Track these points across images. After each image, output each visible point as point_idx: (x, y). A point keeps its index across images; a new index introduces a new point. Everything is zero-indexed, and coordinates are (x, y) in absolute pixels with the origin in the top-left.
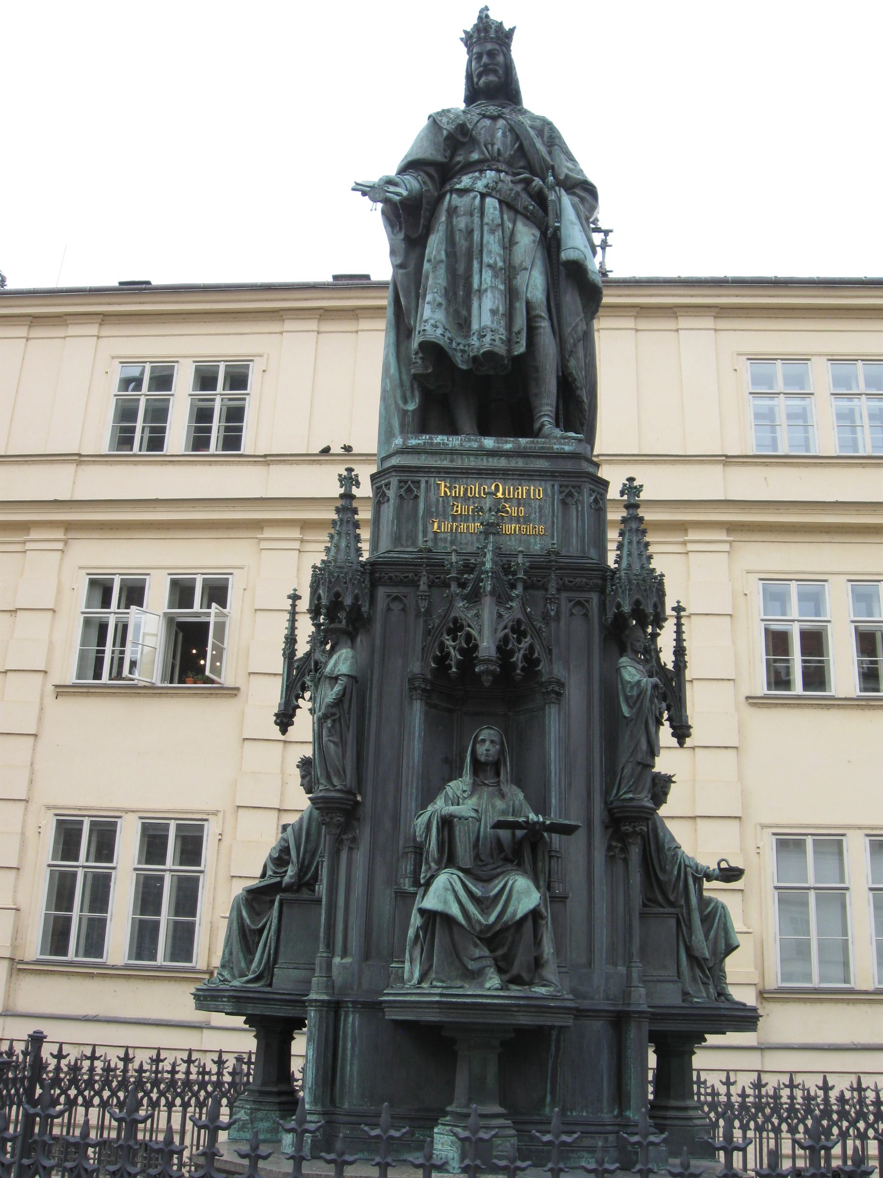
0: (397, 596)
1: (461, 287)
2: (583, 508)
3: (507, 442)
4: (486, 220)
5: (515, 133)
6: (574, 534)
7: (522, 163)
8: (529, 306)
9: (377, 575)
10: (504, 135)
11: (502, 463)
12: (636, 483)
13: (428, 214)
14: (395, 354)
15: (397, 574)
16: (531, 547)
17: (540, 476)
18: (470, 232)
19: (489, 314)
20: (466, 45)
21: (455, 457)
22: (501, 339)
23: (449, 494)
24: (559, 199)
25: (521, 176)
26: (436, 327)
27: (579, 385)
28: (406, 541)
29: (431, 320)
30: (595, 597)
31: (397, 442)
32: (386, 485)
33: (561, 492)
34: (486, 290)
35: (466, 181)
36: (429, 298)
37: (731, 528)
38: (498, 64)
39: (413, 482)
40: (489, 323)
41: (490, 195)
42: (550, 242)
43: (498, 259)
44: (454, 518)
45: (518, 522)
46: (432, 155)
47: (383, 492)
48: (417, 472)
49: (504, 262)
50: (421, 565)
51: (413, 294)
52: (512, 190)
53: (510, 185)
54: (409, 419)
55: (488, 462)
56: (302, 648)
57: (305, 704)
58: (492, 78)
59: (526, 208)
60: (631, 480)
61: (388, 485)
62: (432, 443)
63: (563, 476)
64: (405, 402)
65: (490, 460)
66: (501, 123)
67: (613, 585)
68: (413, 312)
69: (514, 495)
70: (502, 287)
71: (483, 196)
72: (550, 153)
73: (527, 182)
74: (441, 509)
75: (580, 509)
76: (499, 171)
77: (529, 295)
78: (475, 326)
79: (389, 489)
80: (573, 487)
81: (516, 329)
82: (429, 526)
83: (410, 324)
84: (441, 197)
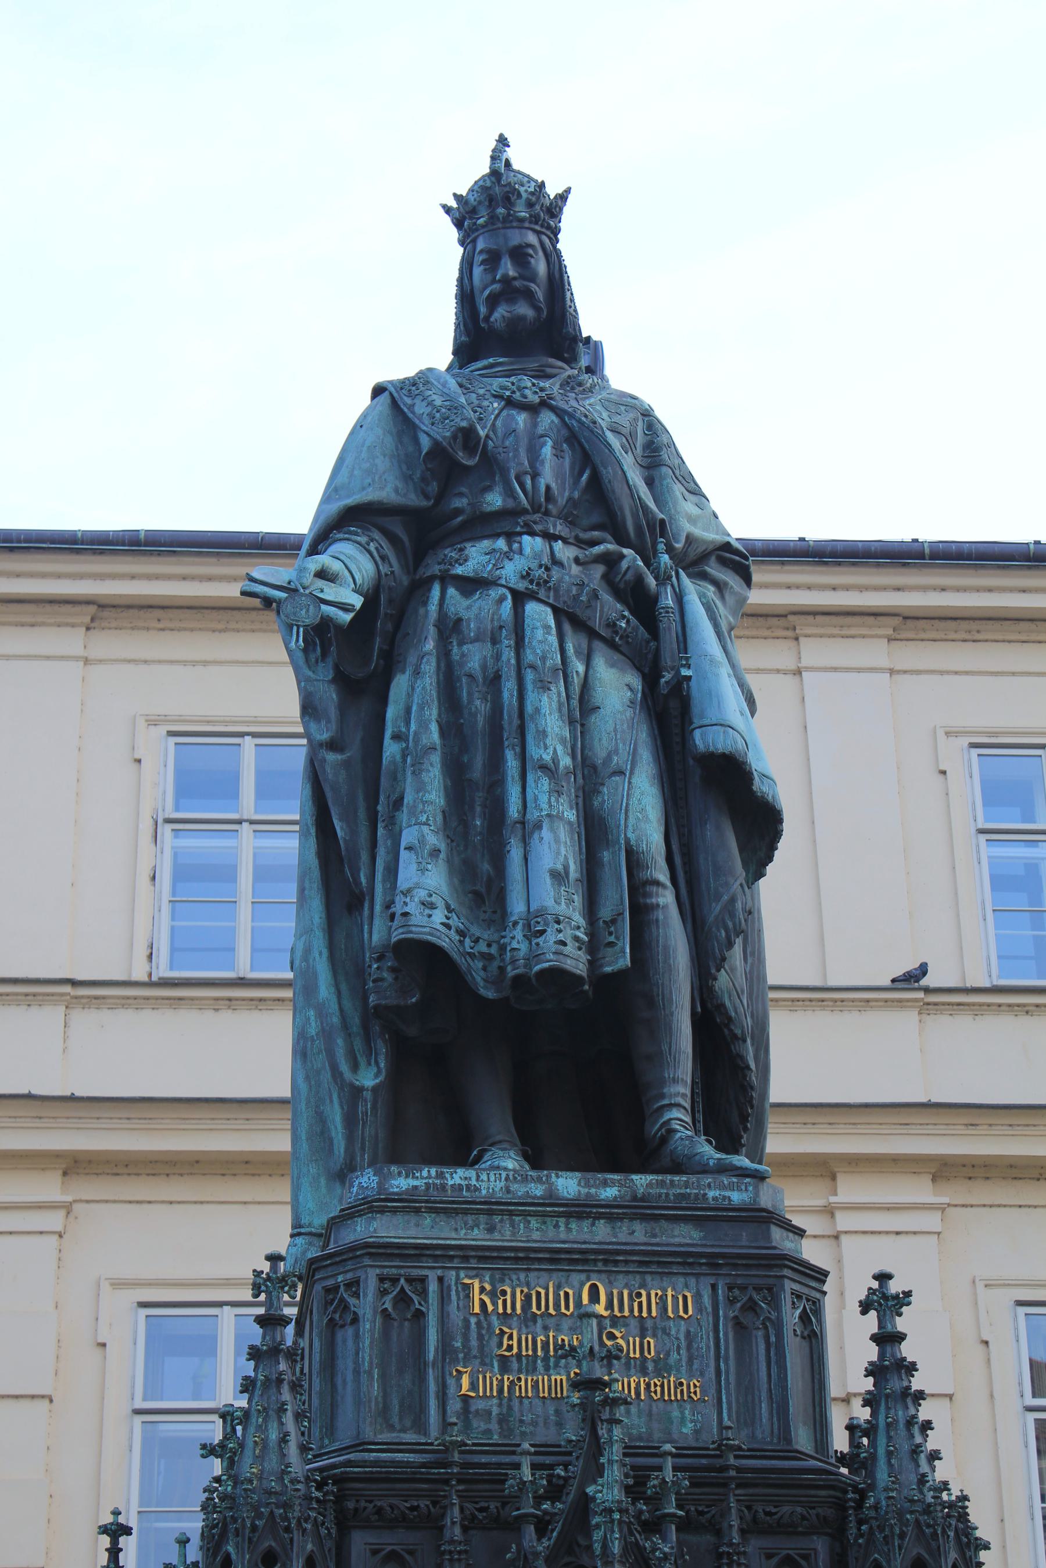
0: (393, 1552)
1: (478, 809)
2: (780, 1336)
3: (605, 1184)
4: (529, 657)
5: (582, 445)
6: (764, 1395)
7: (595, 518)
8: (634, 860)
9: (351, 1505)
10: (558, 454)
11: (601, 1232)
12: (895, 1287)
13: (390, 626)
14: (325, 953)
15: (394, 1501)
16: (674, 1429)
17: (683, 1264)
18: (495, 681)
19: (548, 880)
20: (459, 224)
21: (497, 1219)
22: (576, 939)
23: (490, 1308)
24: (680, 598)
26: (432, 906)
27: (738, 1032)
28: (401, 1419)
29: (424, 892)
30: (820, 1545)
31: (364, 1180)
32: (348, 1286)
33: (731, 1302)
34: (538, 826)
35: (476, 557)
36: (408, 837)
37: (944, 1170)
38: (533, 278)
39: (410, 1280)
40: (550, 903)
41: (533, 596)
42: (669, 708)
43: (560, 749)
45: (644, 1371)
46: (396, 490)
47: (342, 1300)
48: (418, 1257)
49: (574, 757)
50: (446, 1482)
51: (362, 814)
52: (581, 585)
53: (575, 569)
54: (365, 1106)
55: (569, 1230)
58: (524, 310)
59: (612, 625)
60: (883, 1278)
61: (353, 1286)
62: (443, 1187)
63: (735, 1266)
64: (355, 1067)
65: (573, 1226)
66: (547, 419)
67: (860, 1522)
68: (364, 857)
69: (631, 1310)
70: (571, 815)
71: (519, 598)
72: (650, 482)
73: (610, 561)
74: (474, 1343)
75: (773, 1339)
76: (550, 537)
77: (630, 835)
78: (517, 907)
79: (356, 1295)
80: (758, 1289)
81: (605, 913)
82: (451, 1382)
83: (358, 883)
84: (419, 588)
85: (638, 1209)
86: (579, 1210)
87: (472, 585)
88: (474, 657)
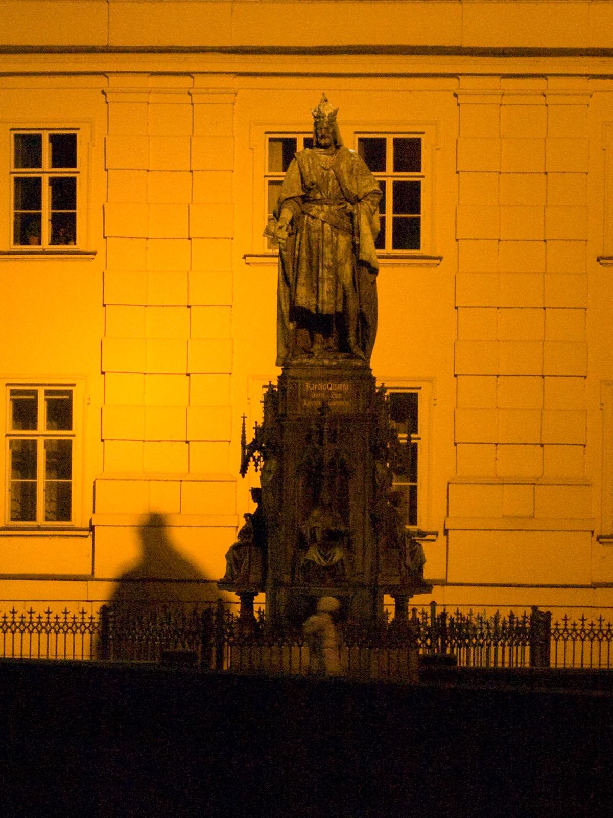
10: (333, 183)
11: (332, 372)
24: (359, 219)
25: (342, 206)
26: (302, 298)
35: (315, 209)
42: (355, 248)
44: (313, 400)
46: (298, 193)
56: (249, 441)
57: (252, 464)
58: (327, 141)
70: (332, 276)
71: (323, 222)
73: (345, 208)
76: (331, 205)
78: (320, 298)
81: (338, 298)
85: (339, 367)
86: (329, 367)
87: (313, 218)
88: (314, 236)
